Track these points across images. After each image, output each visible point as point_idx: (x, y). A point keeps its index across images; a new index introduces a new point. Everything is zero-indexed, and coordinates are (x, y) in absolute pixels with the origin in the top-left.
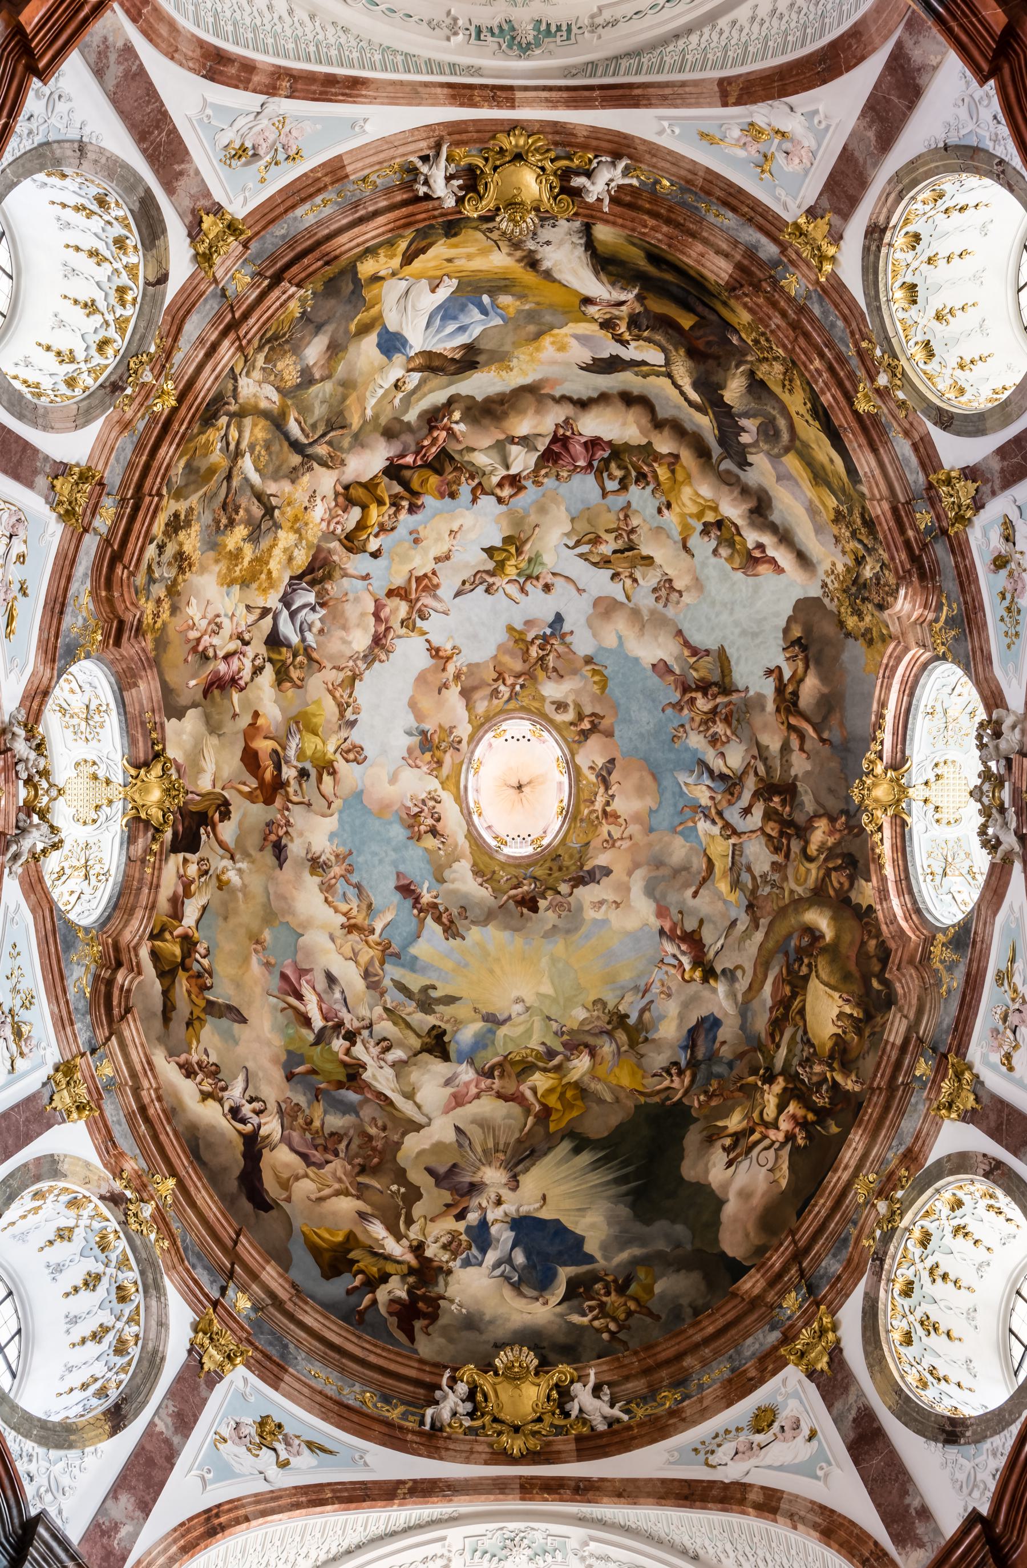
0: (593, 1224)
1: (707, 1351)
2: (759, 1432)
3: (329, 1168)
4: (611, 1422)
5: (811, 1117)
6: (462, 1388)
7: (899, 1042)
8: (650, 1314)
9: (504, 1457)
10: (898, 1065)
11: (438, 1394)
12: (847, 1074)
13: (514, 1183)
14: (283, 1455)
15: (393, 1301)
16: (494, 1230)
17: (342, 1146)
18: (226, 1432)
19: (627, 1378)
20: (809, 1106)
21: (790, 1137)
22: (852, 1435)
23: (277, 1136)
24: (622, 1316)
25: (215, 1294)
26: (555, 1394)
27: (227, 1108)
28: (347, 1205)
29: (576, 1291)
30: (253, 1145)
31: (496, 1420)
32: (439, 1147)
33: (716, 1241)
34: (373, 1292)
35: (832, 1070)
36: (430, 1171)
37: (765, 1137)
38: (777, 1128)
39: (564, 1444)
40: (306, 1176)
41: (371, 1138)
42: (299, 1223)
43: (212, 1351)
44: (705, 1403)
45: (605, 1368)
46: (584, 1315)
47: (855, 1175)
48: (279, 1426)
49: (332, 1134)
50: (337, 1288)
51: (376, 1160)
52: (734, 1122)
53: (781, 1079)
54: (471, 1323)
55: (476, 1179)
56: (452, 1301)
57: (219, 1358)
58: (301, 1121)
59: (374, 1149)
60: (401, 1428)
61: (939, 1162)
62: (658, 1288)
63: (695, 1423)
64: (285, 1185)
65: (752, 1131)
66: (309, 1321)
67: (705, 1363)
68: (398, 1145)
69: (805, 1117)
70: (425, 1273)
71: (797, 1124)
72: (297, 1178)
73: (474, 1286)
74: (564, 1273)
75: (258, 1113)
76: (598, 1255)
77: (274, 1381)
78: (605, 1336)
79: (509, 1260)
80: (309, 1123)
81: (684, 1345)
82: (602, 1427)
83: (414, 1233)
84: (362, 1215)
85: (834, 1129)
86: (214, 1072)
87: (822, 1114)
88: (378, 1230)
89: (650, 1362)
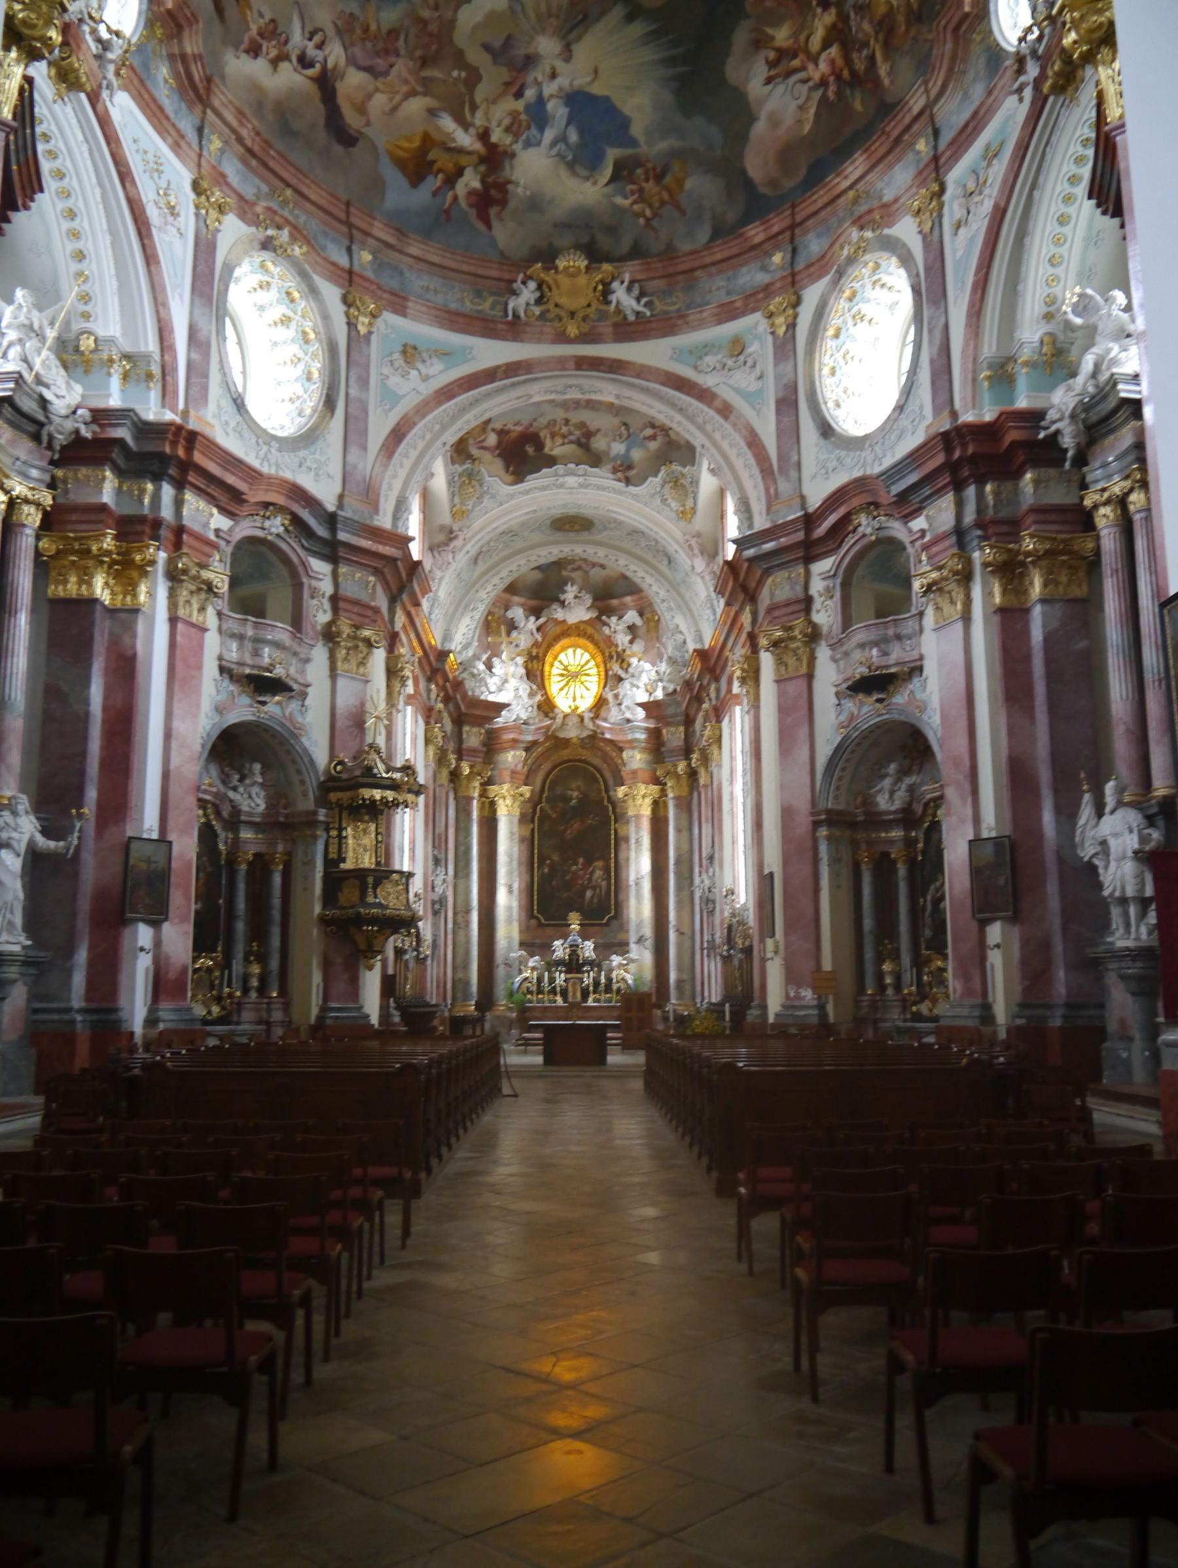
0: (641, 104)
1: (713, 269)
2: (732, 356)
3: (394, 71)
4: (638, 313)
5: (846, 73)
6: (532, 285)
7: (916, 110)
8: (678, 207)
9: (562, 338)
10: (908, 128)
11: (515, 285)
12: (887, 58)
13: (567, 54)
14: (424, 370)
15: (472, 193)
16: (550, 106)
17: (401, 43)
18: (386, 371)
19: (653, 279)
20: (848, 61)
21: (823, 83)
22: (781, 394)
23: (343, 61)
24: (657, 204)
25: (344, 261)
26: (600, 287)
27: (294, 59)
28: (416, 106)
29: (622, 173)
30: (326, 83)
31: (557, 305)
32: (493, 18)
33: (741, 156)
34: (452, 187)
35: (877, 40)
36: (487, 47)
37: (803, 68)
38: (817, 65)
39: (606, 328)
40: (377, 90)
41: (424, 23)
42: (381, 143)
43: (361, 319)
44: (705, 315)
45: (638, 268)
46: (626, 198)
47: (851, 187)
48: (415, 348)
49: (390, 32)
50: (423, 195)
51: (434, 47)
52: (782, 35)
53: (833, 11)
54: (535, 204)
55: (530, 51)
56: (517, 184)
57: (366, 321)
58: (358, 31)
59: (430, 35)
60: (492, 321)
61: (897, 240)
62: (689, 183)
63: (694, 328)
64: (362, 110)
65: (795, 56)
66: (414, 250)
67: (710, 275)
68: (452, 23)
69: (841, 70)
70: (494, 158)
71: (833, 73)
72: (370, 96)
73: (534, 167)
74: (612, 154)
75: (320, 46)
76: (642, 140)
77: (401, 311)
78: (642, 221)
79: (562, 138)
80: (366, 29)
81: (697, 264)
82: (631, 318)
83: (479, 120)
84: (432, 112)
85: (858, 106)
86: (272, 31)
87: (857, 81)
88: (448, 123)
89: (671, 270)
